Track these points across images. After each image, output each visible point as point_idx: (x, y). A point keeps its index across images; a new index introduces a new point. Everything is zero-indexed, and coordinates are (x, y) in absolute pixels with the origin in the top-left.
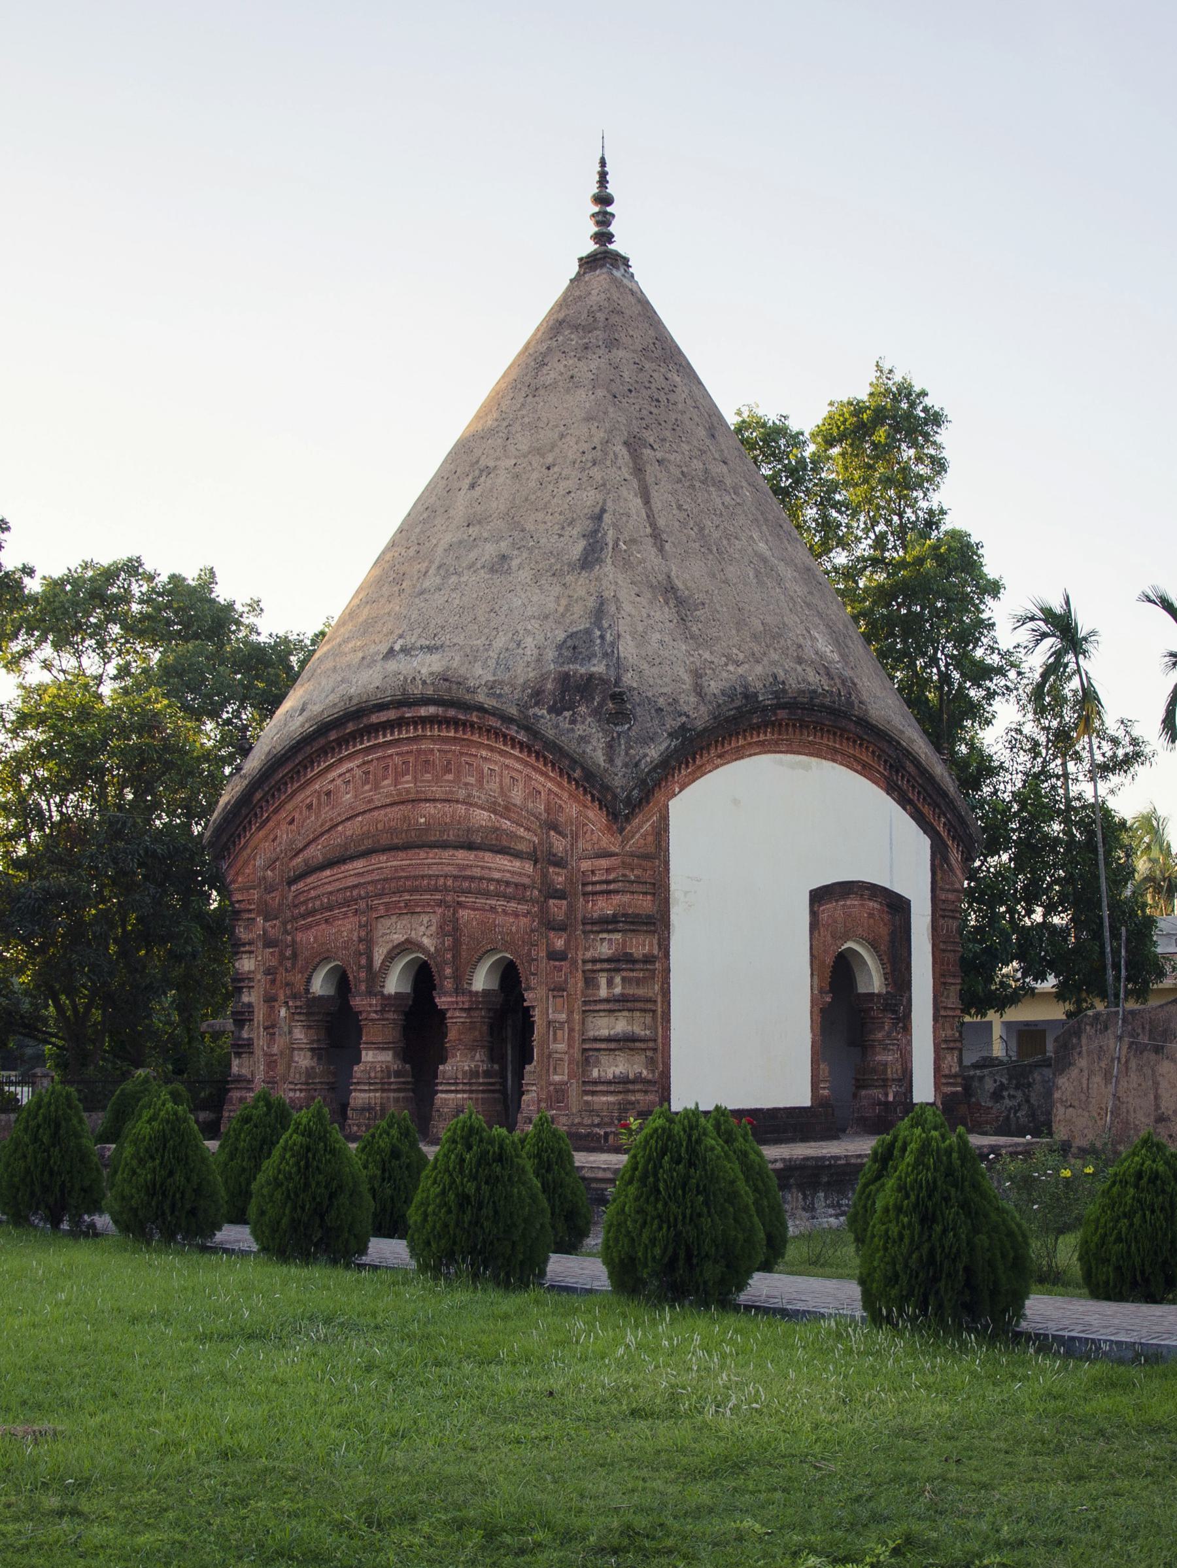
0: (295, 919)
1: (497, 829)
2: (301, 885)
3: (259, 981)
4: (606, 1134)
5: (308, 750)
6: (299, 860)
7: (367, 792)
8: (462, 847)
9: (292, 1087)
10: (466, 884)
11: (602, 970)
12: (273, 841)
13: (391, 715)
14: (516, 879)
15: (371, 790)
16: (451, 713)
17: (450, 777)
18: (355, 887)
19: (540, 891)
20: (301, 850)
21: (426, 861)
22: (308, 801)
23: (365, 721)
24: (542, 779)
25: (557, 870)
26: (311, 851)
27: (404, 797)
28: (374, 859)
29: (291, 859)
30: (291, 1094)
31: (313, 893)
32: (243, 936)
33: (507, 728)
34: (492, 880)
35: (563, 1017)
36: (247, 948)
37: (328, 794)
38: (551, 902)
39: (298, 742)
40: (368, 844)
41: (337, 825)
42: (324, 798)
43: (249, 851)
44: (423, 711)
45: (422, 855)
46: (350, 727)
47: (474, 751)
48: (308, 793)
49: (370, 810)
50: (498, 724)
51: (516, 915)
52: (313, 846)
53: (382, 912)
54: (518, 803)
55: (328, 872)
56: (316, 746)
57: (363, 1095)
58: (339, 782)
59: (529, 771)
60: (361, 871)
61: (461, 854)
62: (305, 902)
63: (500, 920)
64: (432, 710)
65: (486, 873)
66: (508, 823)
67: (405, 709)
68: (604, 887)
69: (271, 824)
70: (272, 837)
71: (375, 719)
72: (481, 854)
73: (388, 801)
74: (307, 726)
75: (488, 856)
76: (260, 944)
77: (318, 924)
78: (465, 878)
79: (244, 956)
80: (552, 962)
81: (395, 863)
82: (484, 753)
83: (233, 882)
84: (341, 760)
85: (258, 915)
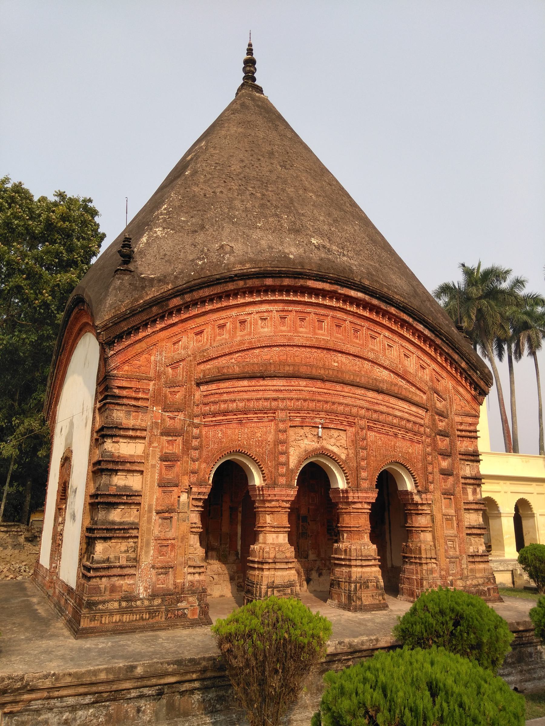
0: (204, 415)
1: (396, 385)
2: (214, 386)
3: (153, 466)
4: (489, 589)
5: (241, 283)
6: (209, 366)
7: (284, 331)
8: (373, 390)
9: (192, 570)
10: (375, 416)
11: (470, 484)
12: (174, 344)
13: (327, 286)
14: (412, 418)
15: (289, 332)
16: (375, 302)
17: (358, 341)
18: (275, 399)
19: (431, 429)
20: (211, 359)
21: (343, 394)
22: (222, 322)
23: (301, 282)
24: (429, 361)
25: (441, 418)
26: (223, 361)
27: (322, 344)
28: (294, 382)
29: (199, 364)
30: (190, 578)
31: (225, 397)
32: (124, 421)
33: (417, 325)
34: (396, 416)
35: (452, 512)
36: (131, 433)
37: (243, 322)
38: (438, 437)
39: (236, 275)
40: (289, 369)
41: (254, 348)
42: (238, 324)
43: (143, 345)
44: (353, 293)
45: (339, 387)
46: (287, 282)
47: (379, 329)
48: (223, 314)
49: (288, 345)
50: (411, 320)
51: (411, 440)
52: (227, 358)
53: (297, 424)
54: (411, 371)
55: (245, 383)
56: (250, 283)
57: (279, 573)
58: (257, 316)
59: (420, 353)
60: (282, 388)
61: (371, 394)
62: (215, 403)
63: (400, 443)
64: (360, 295)
65: (390, 411)
66: (404, 382)
67: (339, 287)
68: (468, 434)
69: (175, 329)
70: (175, 339)
71: (311, 283)
72: (387, 398)
73: (308, 343)
74: (248, 266)
75: (393, 400)
76: (157, 432)
77: (229, 421)
78: (376, 411)
79: (121, 440)
80: (442, 476)
81: (314, 389)
82: (387, 334)
83: (117, 368)
84: (262, 302)
85: (156, 403)
